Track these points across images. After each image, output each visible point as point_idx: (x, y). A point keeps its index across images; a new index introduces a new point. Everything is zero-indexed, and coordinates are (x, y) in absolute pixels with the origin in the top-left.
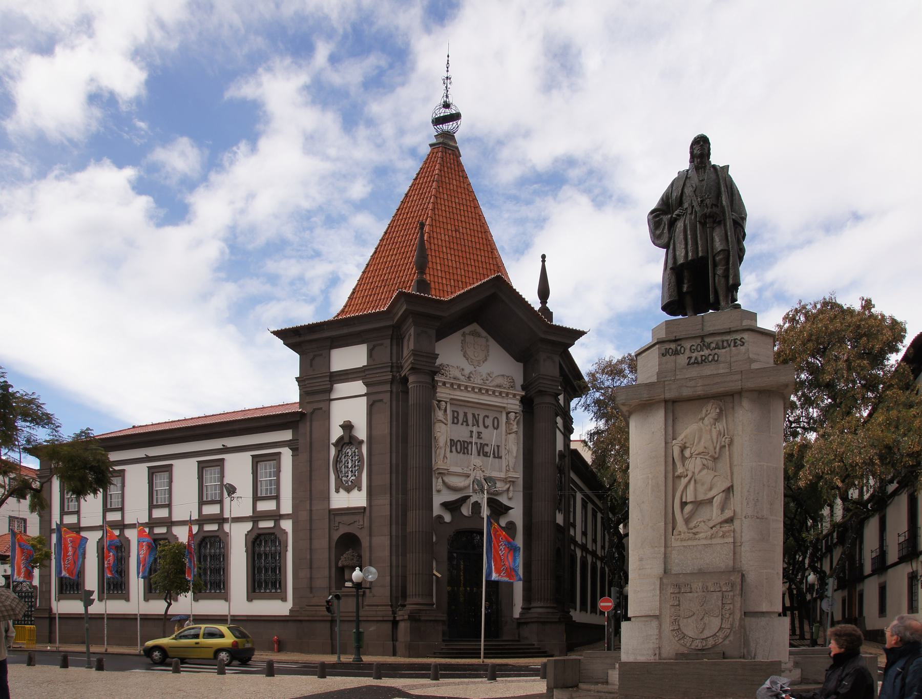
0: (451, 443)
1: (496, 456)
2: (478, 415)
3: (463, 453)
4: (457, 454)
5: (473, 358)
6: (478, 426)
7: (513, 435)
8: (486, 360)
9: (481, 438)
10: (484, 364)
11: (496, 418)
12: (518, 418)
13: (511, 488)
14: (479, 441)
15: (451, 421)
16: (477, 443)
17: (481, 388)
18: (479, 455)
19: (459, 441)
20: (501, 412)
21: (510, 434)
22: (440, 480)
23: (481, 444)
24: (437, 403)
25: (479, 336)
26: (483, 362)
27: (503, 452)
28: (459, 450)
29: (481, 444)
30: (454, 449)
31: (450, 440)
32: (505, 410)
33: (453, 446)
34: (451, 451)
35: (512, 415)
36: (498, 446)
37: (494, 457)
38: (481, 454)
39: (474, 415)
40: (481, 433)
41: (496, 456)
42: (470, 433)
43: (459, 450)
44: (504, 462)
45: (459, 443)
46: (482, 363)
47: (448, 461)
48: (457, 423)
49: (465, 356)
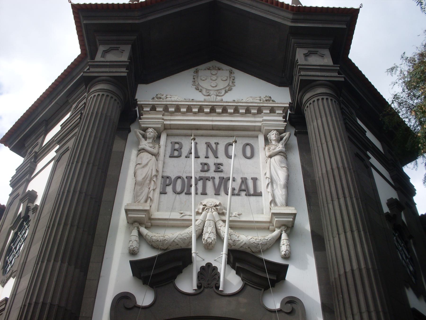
1: (252, 192)
2: (217, 144)
3: (186, 194)
4: (175, 195)
5: (211, 88)
6: (217, 158)
7: (277, 158)
8: (230, 90)
9: (221, 171)
10: (227, 94)
11: (248, 144)
12: (285, 138)
13: (284, 236)
14: (217, 176)
15: (168, 154)
16: (213, 178)
18: (217, 193)
19: (179, 177)
20: (257, 137)
21: (270, 157)
22: (135, 232)
23: (221, 179)
24: (142, 132)
25: (219, 69)
26: (226, 92)
27: (262, 186)
28: (179, 189)
29: (221, 179)
30: (169, 189)
31: (163, 177)
32: (263, 133)
33: (168, 185)
34: (163, 192)
35: (273, 136)
36: (255, 180)
37: (248, 195)
38: (222, 192)
39: (208, 145)
40: (221, 164)
41: (252, 192)
42: (201, 166)
43: (179, 189)
44: (266, 198)
45: (179, 182)
46: (223, 92)
47: (154, 205)
48: (179, 156)
49: (197, 89)
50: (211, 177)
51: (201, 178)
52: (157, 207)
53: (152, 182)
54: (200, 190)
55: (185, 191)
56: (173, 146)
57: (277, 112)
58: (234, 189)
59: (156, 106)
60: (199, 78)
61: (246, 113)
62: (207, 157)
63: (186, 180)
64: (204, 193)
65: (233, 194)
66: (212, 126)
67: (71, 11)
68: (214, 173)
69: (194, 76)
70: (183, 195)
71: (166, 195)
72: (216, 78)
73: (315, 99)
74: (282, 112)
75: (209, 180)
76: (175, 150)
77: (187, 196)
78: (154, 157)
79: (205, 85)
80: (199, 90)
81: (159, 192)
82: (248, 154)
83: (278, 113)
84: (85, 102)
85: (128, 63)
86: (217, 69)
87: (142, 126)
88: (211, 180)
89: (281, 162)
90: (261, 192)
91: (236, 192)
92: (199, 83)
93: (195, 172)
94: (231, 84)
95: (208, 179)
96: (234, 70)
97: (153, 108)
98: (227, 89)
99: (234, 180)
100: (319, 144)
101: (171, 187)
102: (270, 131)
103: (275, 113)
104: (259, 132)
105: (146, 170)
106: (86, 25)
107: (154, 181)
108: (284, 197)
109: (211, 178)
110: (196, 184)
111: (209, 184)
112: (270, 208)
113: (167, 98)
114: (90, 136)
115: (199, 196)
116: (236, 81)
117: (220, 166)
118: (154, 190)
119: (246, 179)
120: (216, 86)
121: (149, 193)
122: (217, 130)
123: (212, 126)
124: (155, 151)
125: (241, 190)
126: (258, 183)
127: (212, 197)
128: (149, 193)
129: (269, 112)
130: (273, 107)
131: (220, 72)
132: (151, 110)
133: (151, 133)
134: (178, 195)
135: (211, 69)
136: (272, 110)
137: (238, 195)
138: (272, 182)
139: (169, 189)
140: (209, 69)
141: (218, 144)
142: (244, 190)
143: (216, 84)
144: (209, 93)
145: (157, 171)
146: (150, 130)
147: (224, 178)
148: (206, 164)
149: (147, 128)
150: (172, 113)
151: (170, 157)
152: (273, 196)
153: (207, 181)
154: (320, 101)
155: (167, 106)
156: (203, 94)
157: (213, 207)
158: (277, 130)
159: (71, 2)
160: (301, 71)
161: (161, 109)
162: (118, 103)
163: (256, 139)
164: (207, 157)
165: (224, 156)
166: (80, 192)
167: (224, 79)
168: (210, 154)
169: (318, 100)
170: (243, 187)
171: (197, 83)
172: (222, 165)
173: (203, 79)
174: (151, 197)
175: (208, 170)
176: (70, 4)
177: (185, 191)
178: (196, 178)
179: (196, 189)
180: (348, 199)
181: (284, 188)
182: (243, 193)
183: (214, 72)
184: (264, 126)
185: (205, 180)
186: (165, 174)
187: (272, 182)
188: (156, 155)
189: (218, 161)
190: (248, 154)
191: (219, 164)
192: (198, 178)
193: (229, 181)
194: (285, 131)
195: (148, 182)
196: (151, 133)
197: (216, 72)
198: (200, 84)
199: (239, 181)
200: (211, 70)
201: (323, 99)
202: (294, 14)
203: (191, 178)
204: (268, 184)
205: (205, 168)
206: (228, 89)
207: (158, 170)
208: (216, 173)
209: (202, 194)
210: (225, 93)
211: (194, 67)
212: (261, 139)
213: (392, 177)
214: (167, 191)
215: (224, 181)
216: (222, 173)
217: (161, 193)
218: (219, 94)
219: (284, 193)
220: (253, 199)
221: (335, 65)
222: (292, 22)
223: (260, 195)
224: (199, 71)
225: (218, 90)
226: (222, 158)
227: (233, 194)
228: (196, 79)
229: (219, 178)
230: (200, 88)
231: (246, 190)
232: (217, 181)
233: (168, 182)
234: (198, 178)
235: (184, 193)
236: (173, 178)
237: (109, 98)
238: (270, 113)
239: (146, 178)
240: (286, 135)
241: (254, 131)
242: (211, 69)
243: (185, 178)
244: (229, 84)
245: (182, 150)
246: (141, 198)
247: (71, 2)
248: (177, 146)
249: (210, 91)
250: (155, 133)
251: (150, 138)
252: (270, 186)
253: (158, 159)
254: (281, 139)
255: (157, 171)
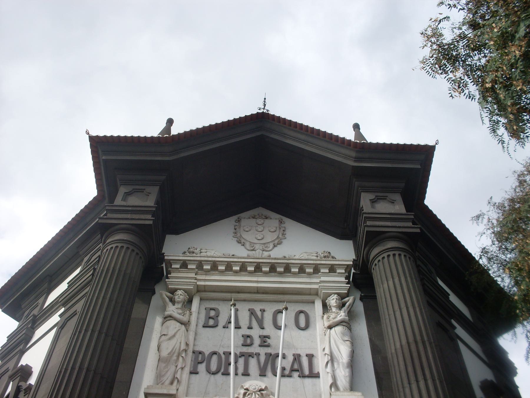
0: (196, 358)
1: (307, 372)
2: (263, 311)
3: (223, 374)
4: (209, 375)
5: (256, 241)
6: (263, 328)
7: (339, 329)
8: (280, 243)
9: (268, 346)
10: (276, 249)
11: (301, 312)
12: (348, 304)
14: (263, 351)
15: (201, 323)
16: (258, 355)
17: (259, 263)
18: (263, 374)
19: (215, 353)
20: (313, 302)
21: (330, 327)
25: (267, 218)
26: (275, 246)
28: (214, 367)
29: (269, 355)
30: (202, 368)
31: (194, 352)
32: (320, 298)
33: (201, 363)
34: (194, 372)
35: (333, 301)
36: (311, 357)
38: (269, 373)
39: (252, 312)
40: (268, 337)
41: (307, 372)
42: (242, 339)
43: (214, 367)
44: (325, 380)
45: (215, 358)
46: (271, 246)
47: (182, 388)
48: (215, 326)
49: (239, 242)
50: (255, 353)
51: (242, 355)
52: (185, 391)
53: (181, 359)
54: (241, 370)
55: (222, 370)
56: (207, 313)
57: (338, 271)
58: (283, 369)
59: (187, 262)
60: (242, 229)
61: (299, 272)
62: (250, 328)
63: (223, 356)
64: (246, 374)
65: (283, 376)
66: (257, 288)
67: (88, 143)
68: (259, 348)
69: (235, 226)
70: (219, 376)
71: (197, 375)
72: (262, 228)
73: (385, 255)
74: (344, 271)
75: (253, 357)
76: (210, 318)
77: (224, 377)
78: (183, 326)
79: (249, 237)
80: (241, 243)
81: (188, 372)
82: (302, 324)
83: (339, 273)
84: (100, 254)
85: (154, 209)
86: (264, 217)
87: (169, 287)
88: (255, 357)
89: (343, 334)
90: (318, 373)
91: (287, 372)
92: (241, 235)
93: (235, 347)
94: (281, 236)
95: (251, 355)
96: (285, 219)
97: (184, 265)
98: (276, 242)
99: (284, 357)
100: (391, 312)
101: (204, 365)
102: (330, 295)
103: (336, 272)
104: (316, 297)
105: (173, 342)
106: (105, 161)
107: (182, 357)
108: (348, 379)
109: (256, 354)
110: (236, 362)
111: (253, 362)
112: (330, 393)
113: (201, 252)
114: (104, 298)
115: (240, 377)
116: (288, 233)
117: (267, 339)
118: (182, 368)
119: (299, 356)
120: (263, 239)
121: (176, 372)
122: (263, 293)
123: (257, 288)
124: (185, 319)
125: (293, 370)
126: (315, 361)
127: (256, 379)
128: (176, 372)
129: (327, 271)
130: (332, 265)
131: (267, 221)
132: (181, 268)
133: (180, 296)
134: (213, 376)
135: (257, 217)
136: (332, 269)
137: (290, 376)
138: (332, 359)
139: (202, 368)
140: (254, 218)
141: (264, 311)
142: (298, 371)
143: (262, 236)
144: (253, 247)
145: (187, 345)
146: (179, 292)
147: (271, 355)
148: (248, 336)
149: (176, 290)
150: (207, 272)
151: (204, 327)
152: (334, 378)
153: (250, 358)
154: (391, 257)
155: (201, 262)
156: (246, 248)
157: (257, 391)
158: (338, 294)
159: (88, 134)
160: (367, 220)
161: (194, 267)
162: (141, 257)
163: (311, 305)
164: (250, 328)
165: (272, 327)
166: (88, 370)
167: (272, 230)
168: (255, 324)
169: (389, 256)
170: (296, 367)
171: (239, 235)
172: (269, 338)
173: (247, 230)
174: (178, 377)
175: (251, 345)
176: (88, 135)
177: (222, 370)
178: (235, 354)
179: (236, 369)
180: (430, 382)
181: (348, 367)
182: (296, 374)
183: (260, 221)
184: (321, 288)
185: (247, 356)
186: (198, 349)
187: (332, 359)
188: (186, 324)
189: (265, 333)
190: (302, 324)
191: (265, 337)
192: (238, 353)
193: (277, 358)
194: (348, 295)
195: (175, 358)
196: (180, 296)
197: (262, 221)
198: (243, 236)
199: (290, 358)
200: (256, 218)
201: (394, 255)
202: (357, 152)
203: (230, 354)
204: (327, 363)
205: (247, 340)
206: (278, 243)
207: (188, 343)
208: (262, 348)
209: (243, 375)
210: (273, 248)
211: (235, 214)
212: (318, 306)
213: (485, 352)
214: (198, 370)
215: (272, 358)
216: (269, 348)
217: (191, 373)
218: (266, 249)
219: (347, 374)
220: (308, 381)
221: (408, 213)
222: (355, 161)
223: (317, 376)
224: (242, 219)
225: (264, 244)
226: (270, 329)
227: (283, 376)
228: (238, 230)
229: (265, 354)
230: (243, 241)
231: (300, 369)
232: (263, 358)
233: (200, 359)
234: (238, 353)
235: (220, 373)
236: (207, 353)
237: (130, 251)
238: (329, 272)
239: (172, 354)
240: (350, 300)
241: (310, 294)
242: (257, 217)
243: (222, 353)
244: (278, 236)
245: (219, 318)
246: (165, 378)
247: (88, 134)
248: (212, 313)
249: (255, 245)
250: (185, 296)
251: (178, 302)
252: (329, 365)
253: (189, 330)
254: (344, 305)
255: (187, 345)
